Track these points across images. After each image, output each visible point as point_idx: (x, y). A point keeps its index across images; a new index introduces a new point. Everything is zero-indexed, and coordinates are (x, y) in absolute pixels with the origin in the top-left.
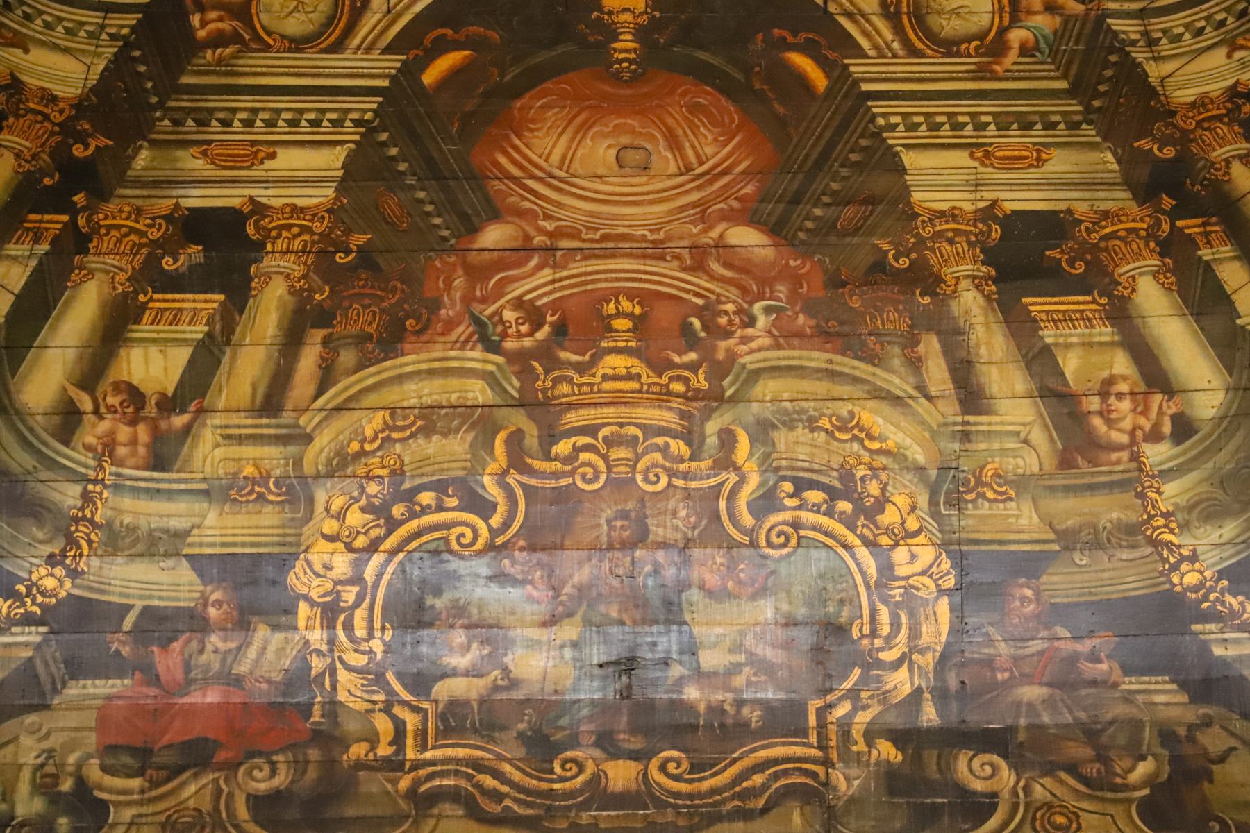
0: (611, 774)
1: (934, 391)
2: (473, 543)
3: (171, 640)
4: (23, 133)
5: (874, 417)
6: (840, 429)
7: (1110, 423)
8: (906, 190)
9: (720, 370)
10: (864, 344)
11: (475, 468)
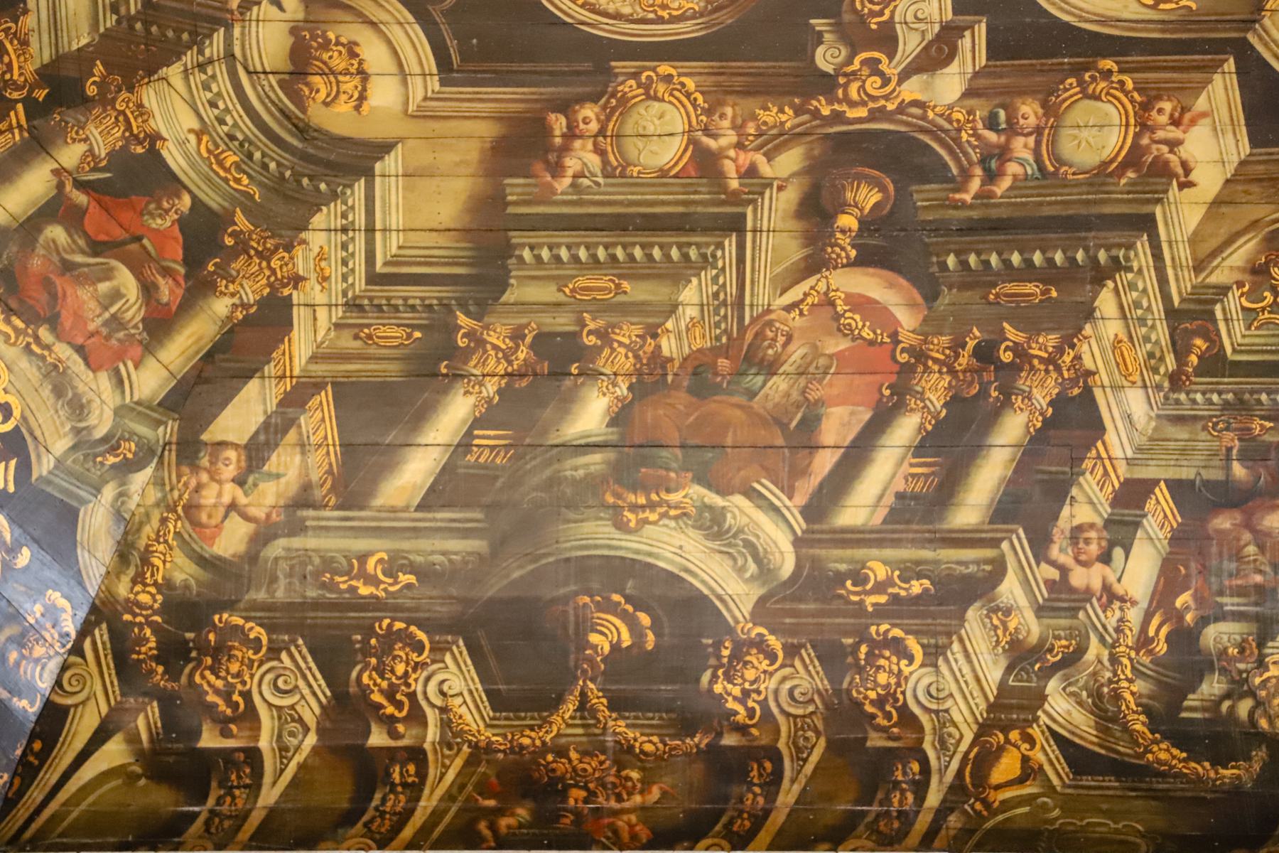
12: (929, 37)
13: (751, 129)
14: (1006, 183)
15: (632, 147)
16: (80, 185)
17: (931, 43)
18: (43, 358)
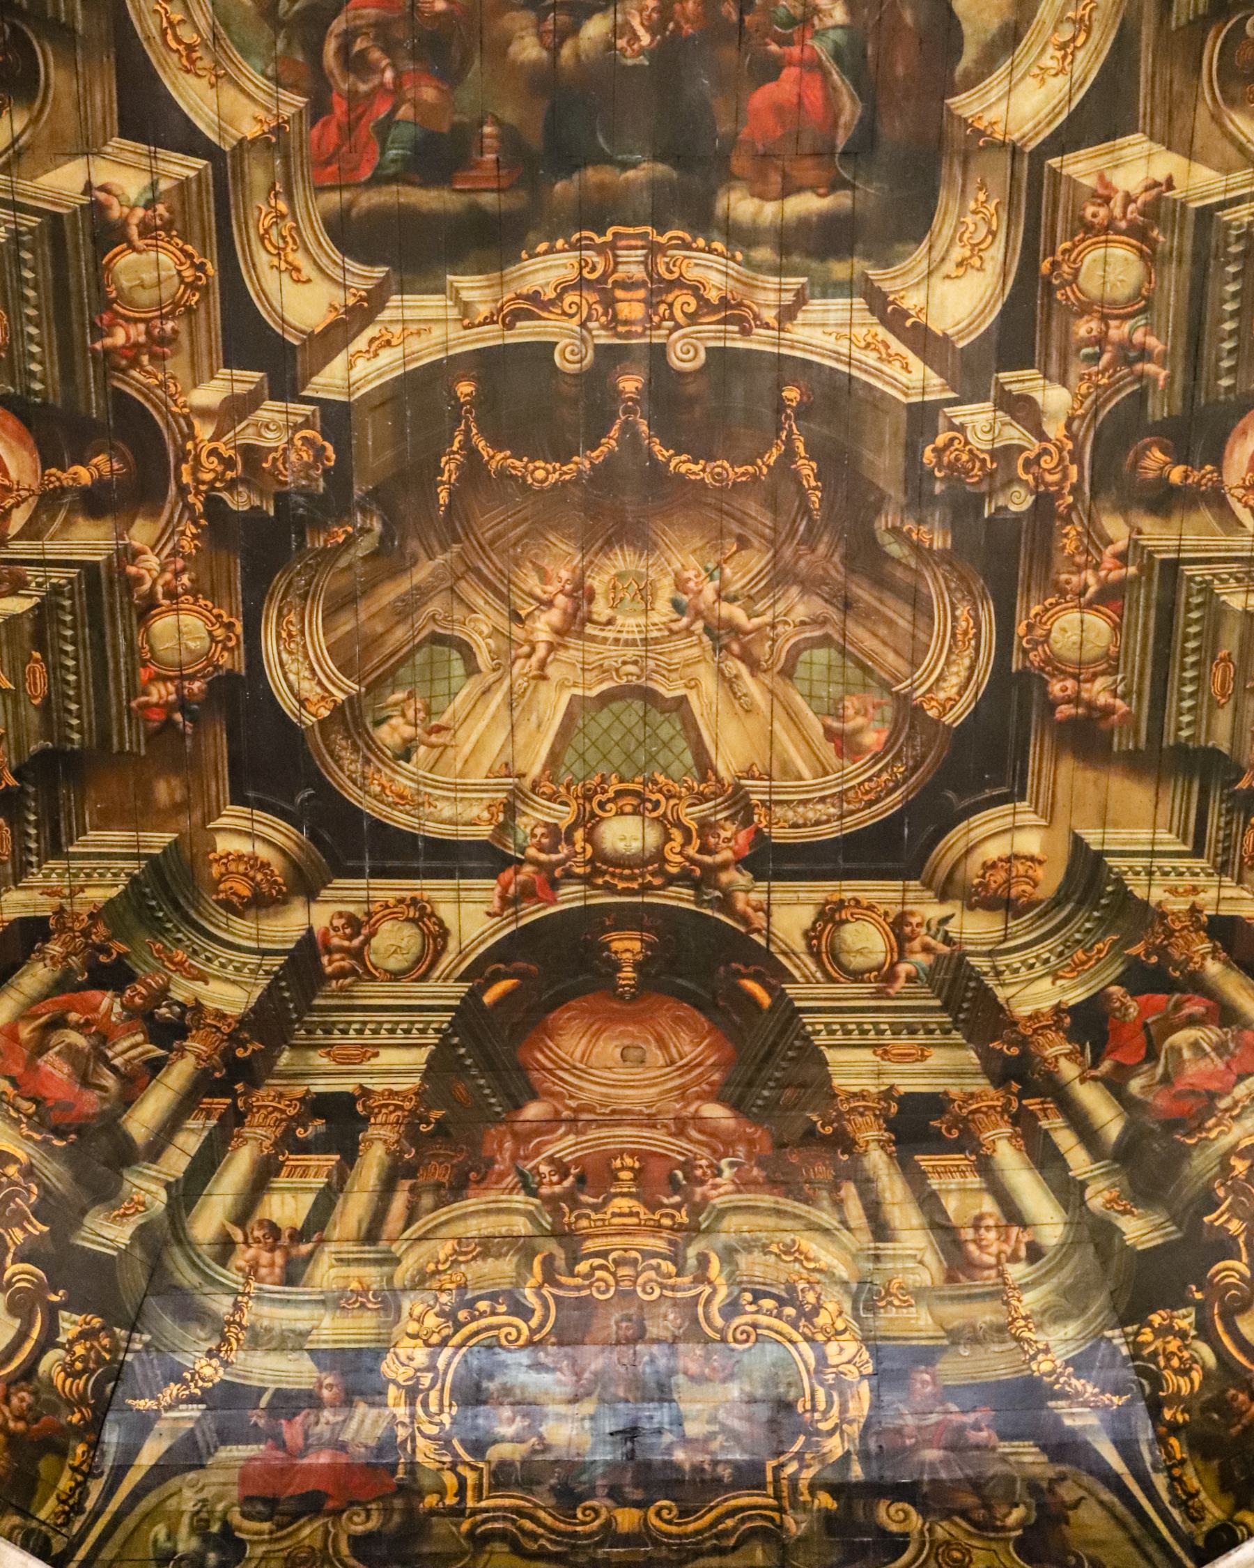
0: (619, 1519)
1: (853, 1224)
2: (517, 1340)
3: (295, 1415)
4: (203, 1041)
5: (811, 1244)
6: (786, 1253)
7: (981, 1248)
8: (828, 1078)
9: (696, 1209)
10: (801, 1189)
11: (519, 1282)
12: (1008, 419)
13: (1080, 559)
14: (1152, 341)
15: (1091, 651)
16: (1095, 1064)
17: (1013, 417)
18: (1244, 1108)
